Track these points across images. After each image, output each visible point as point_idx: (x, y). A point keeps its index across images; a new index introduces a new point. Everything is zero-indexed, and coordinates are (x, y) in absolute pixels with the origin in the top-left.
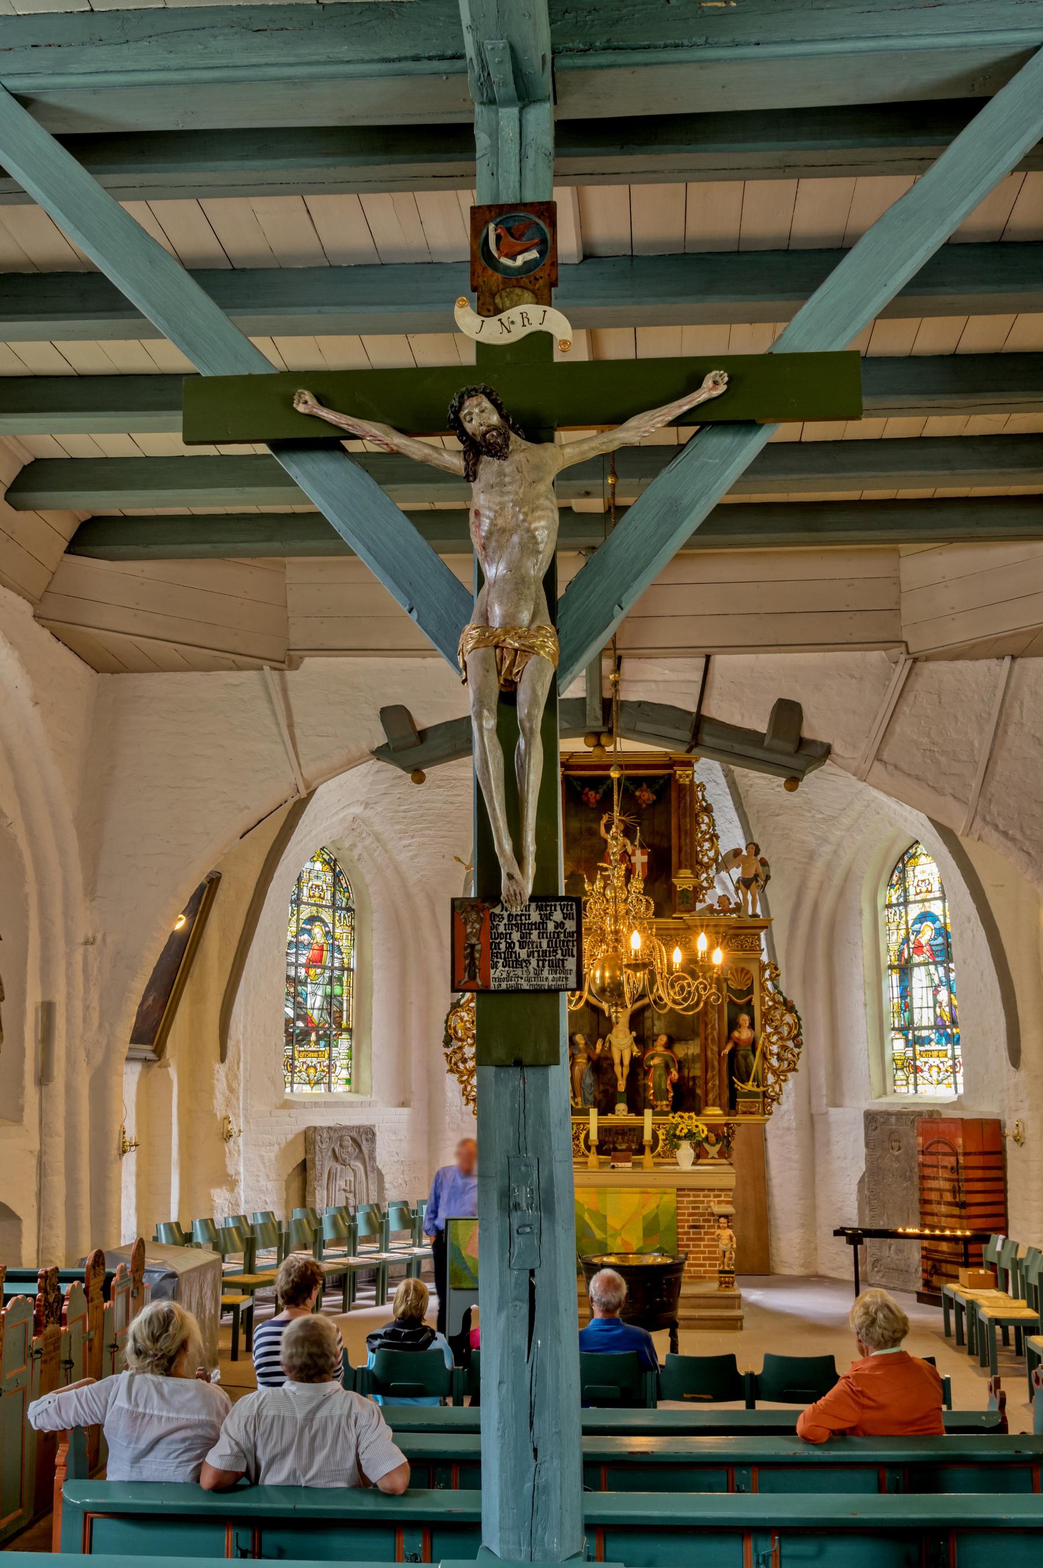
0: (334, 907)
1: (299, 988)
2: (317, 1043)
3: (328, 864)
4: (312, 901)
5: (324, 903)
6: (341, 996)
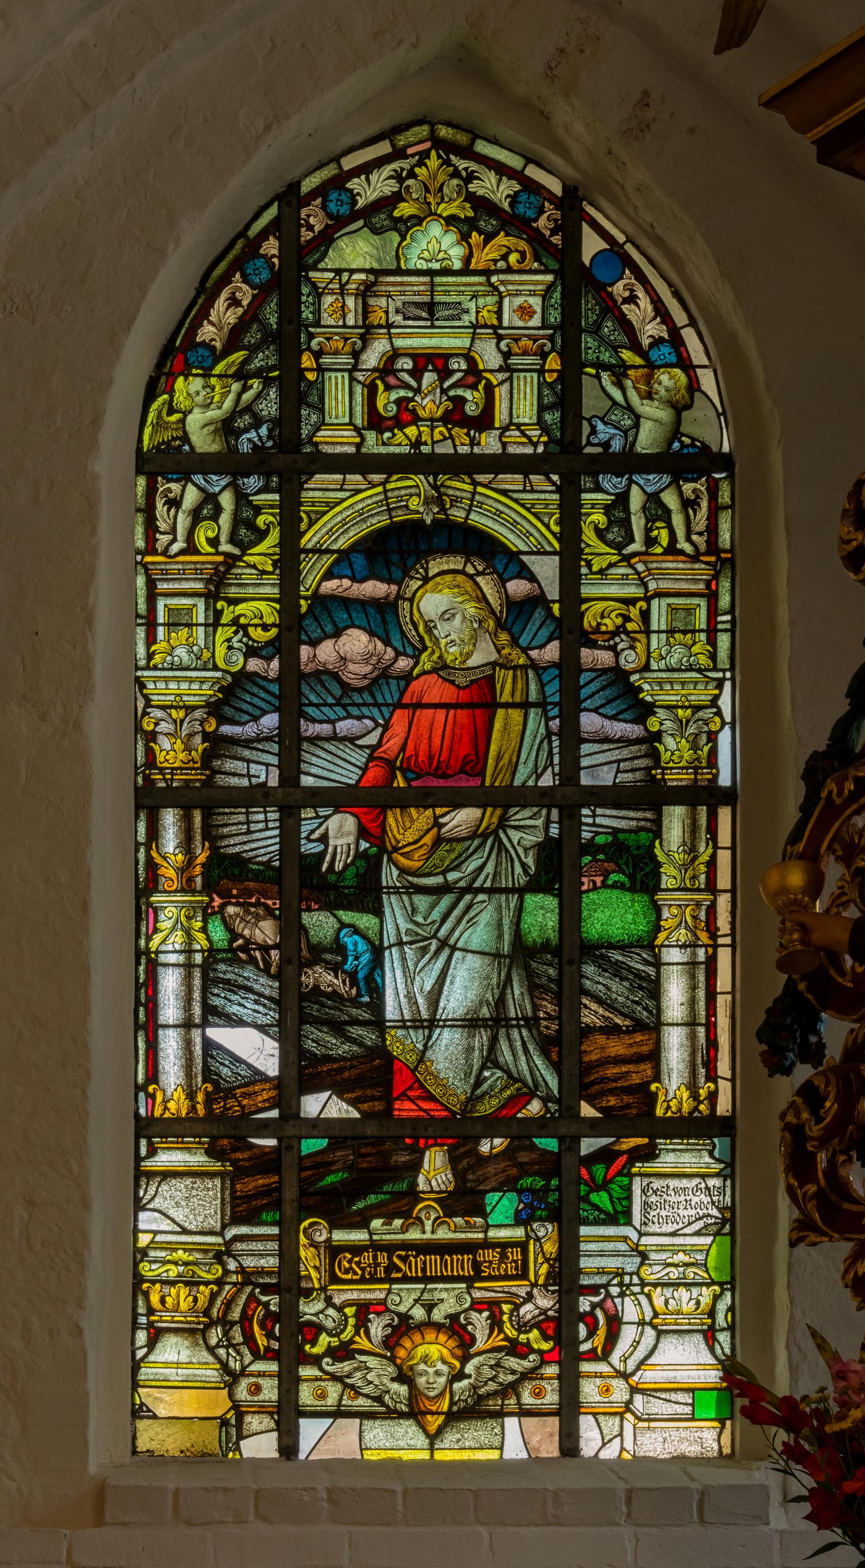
0: (568, 458)
1: (320, 924)
2: (464, 1200)
3: (512, 222)
4: (399, 443)
5: (489, 443)
6: (648, 944)
